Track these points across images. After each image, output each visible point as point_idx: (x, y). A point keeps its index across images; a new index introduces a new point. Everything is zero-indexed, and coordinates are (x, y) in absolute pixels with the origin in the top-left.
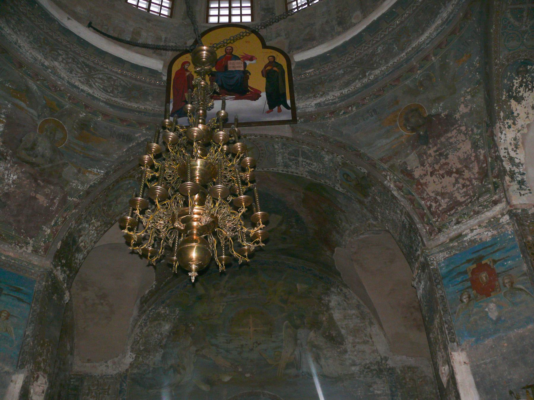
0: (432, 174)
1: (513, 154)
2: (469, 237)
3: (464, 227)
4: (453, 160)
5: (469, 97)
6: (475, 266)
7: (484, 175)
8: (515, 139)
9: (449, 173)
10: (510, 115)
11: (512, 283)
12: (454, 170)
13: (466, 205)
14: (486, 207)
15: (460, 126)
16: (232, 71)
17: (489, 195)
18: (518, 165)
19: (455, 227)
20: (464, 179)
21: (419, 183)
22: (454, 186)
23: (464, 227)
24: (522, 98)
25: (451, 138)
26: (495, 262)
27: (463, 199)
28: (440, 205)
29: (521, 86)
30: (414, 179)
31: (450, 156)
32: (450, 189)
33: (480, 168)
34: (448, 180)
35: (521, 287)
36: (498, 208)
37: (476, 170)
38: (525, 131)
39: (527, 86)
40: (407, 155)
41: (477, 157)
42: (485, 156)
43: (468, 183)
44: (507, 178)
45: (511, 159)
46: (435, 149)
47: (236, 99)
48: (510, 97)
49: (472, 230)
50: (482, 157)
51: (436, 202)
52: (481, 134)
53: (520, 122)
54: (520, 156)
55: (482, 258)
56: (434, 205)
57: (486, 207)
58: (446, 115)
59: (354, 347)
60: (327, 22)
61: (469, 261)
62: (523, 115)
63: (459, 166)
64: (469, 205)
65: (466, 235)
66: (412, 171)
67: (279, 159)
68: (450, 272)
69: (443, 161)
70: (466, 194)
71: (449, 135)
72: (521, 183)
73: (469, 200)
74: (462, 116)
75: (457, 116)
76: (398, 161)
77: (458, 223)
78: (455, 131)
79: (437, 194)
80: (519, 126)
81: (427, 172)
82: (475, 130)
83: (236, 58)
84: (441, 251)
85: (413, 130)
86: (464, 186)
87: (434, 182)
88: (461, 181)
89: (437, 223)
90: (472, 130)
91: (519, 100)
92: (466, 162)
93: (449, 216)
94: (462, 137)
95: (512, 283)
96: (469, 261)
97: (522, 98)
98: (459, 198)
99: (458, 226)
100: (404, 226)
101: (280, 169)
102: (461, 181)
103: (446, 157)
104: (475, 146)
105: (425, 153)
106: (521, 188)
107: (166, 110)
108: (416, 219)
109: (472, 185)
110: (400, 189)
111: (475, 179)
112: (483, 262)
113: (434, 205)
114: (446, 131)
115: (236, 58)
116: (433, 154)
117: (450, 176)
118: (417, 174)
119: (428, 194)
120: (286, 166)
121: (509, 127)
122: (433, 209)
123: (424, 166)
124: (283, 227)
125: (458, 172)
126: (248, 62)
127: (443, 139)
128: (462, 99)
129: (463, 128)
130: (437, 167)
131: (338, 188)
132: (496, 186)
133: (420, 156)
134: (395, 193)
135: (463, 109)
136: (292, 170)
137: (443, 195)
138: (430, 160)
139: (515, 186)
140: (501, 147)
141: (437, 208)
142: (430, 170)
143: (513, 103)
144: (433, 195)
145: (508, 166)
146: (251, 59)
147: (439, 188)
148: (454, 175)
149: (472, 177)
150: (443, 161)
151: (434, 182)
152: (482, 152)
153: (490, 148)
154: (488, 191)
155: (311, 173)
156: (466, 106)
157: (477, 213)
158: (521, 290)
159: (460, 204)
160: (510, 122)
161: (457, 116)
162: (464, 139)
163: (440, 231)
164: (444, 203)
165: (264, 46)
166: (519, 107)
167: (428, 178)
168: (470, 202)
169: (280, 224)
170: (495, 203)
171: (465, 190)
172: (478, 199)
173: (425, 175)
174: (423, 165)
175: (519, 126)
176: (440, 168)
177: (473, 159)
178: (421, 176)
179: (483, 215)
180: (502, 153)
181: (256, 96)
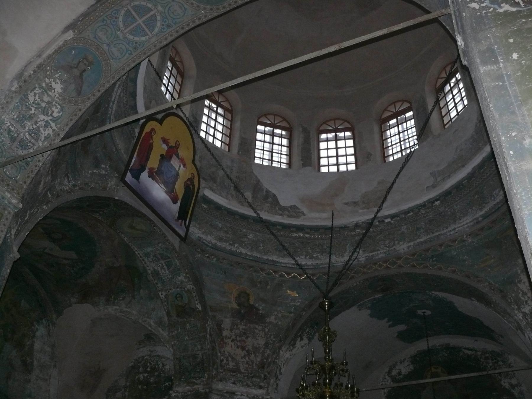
2: (239, 397)
3: (236, 389)
4: (250, 343)
5: (280, 315)
7: (262, 366)
9: (243, 348)
12: (247, 349)
13: (244, 376)
14: (255, 386)
15: (265, 327)
16: (172, 165)
17: (259, 380)
18: (280, 373)
19: (231, 385)
20: (249, 359)
21: (222, 340)
22: (242, 358)
23: (236, 389)
25: (257, 329)
27: (243, 371)
28: (228, 364)
30: (221, 335)
31: (249, 339)
34: (239, 352)
37: (259, 359)
40: (226, 317)
41: (263, 353)
42: (268, 355)
43: (251, 363)
46: (244, 327)
49: (242, 395)
50: (266, 355)
51: (227, 360)
52: (274, 342)
53: (294, 351)
56: (225, 361)
58: (262, 314)
59: (37, 380)
63: (251, 349)
64: (246, 377)
65: (237, 395)
66: (223, 329)
71: (257, 327)
73: (247, 374)
74: (270, 323)
75: (268, 320)
77: (234, 383)
78: (261, 327)
79: (230, 355)
81: (231, 337)
82: (272, 337)
84: (217, 394)
85: (239, 305)
86: (247, 363)
87: (231, 347)
88: (247, 358)
89: (222, 374)
90: (271, 335)
92: (256, 349)
93: (231, 375)
98: (241, 368)
99: (234, 386)
102: (247, 358)
103: (247, 337)
104: (266, 345)
105: (237, 325)
109: (253, 366)
111: (256, 364)
113: (225, 361)
116: (241, 329)
117: (242, 351)
118: (225, 333)
119: (224, 351)
122: (223, 363)
123: (231, 332)
125: (248, 351)
127: (252, 326)
128: (276, 313)
129: (267, 330)
130: (238, 339)
132: (265, 378)
135: (273, 318)
137: (232, 358)
138: (237, 331)
142: (234, 337)
144: (227, 354)
148: (245, 351)
149: (255, 361)
151: (231, 347)
152: (268, 352)
153: (274, 353)
154: (259, 377)
156: (276, 319)
157: (248, 386)
159: (241, 373)
161: (268, 320)
162: (263, 336)
163: (221, 380)
164: (231, 365)
167: (229, 341)
168: (247, 376)
170: (261, 387)
171: (247, 366)
172: (252, 377)
173: (229, 338)
174: (231, 330)
176: (240, 341)
177: (261, 351)
178: (226, 337)
179: (250, 390)
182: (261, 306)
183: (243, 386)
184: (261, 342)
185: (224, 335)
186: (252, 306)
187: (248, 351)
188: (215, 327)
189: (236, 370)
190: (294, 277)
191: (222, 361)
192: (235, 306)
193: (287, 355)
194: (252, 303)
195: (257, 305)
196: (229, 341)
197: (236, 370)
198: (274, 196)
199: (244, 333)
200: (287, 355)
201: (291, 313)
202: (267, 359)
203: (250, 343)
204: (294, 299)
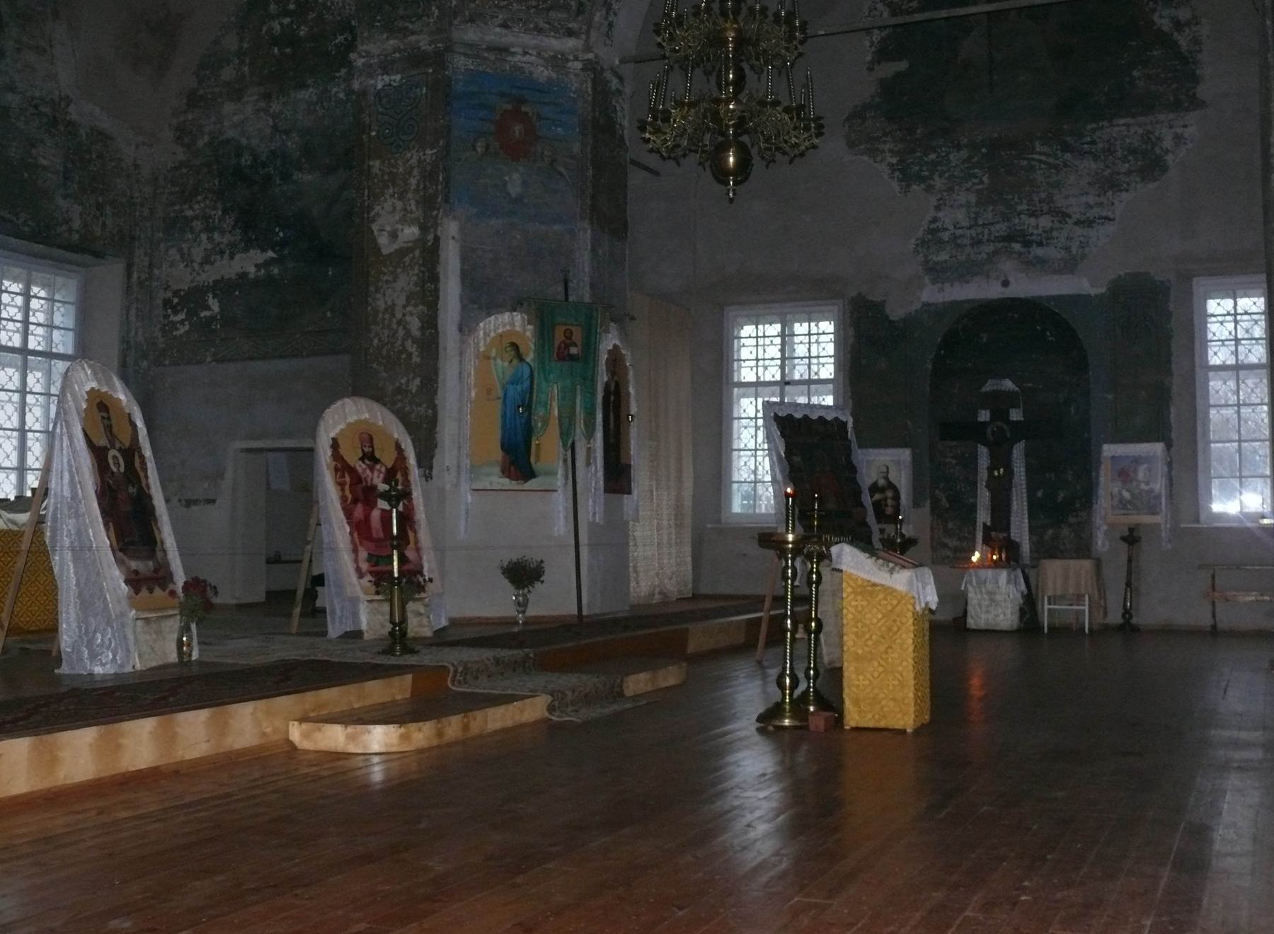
2: (518, 58)
6: (509, 107)
11: (553, 161)
13: (529, 8)
19: (498, 30)
26: (540, 117)
35: (563, 170)
49: (525, 53)
55: (523, 101)
61: (502, 95)
64: (532, 11)
65: (514, 54)
77: (504, 25)
95: (553, 161)
96: (502, 95)
99: (504, 31)
112: (523, 109)
158: (561, 174)
183: (526, 31)
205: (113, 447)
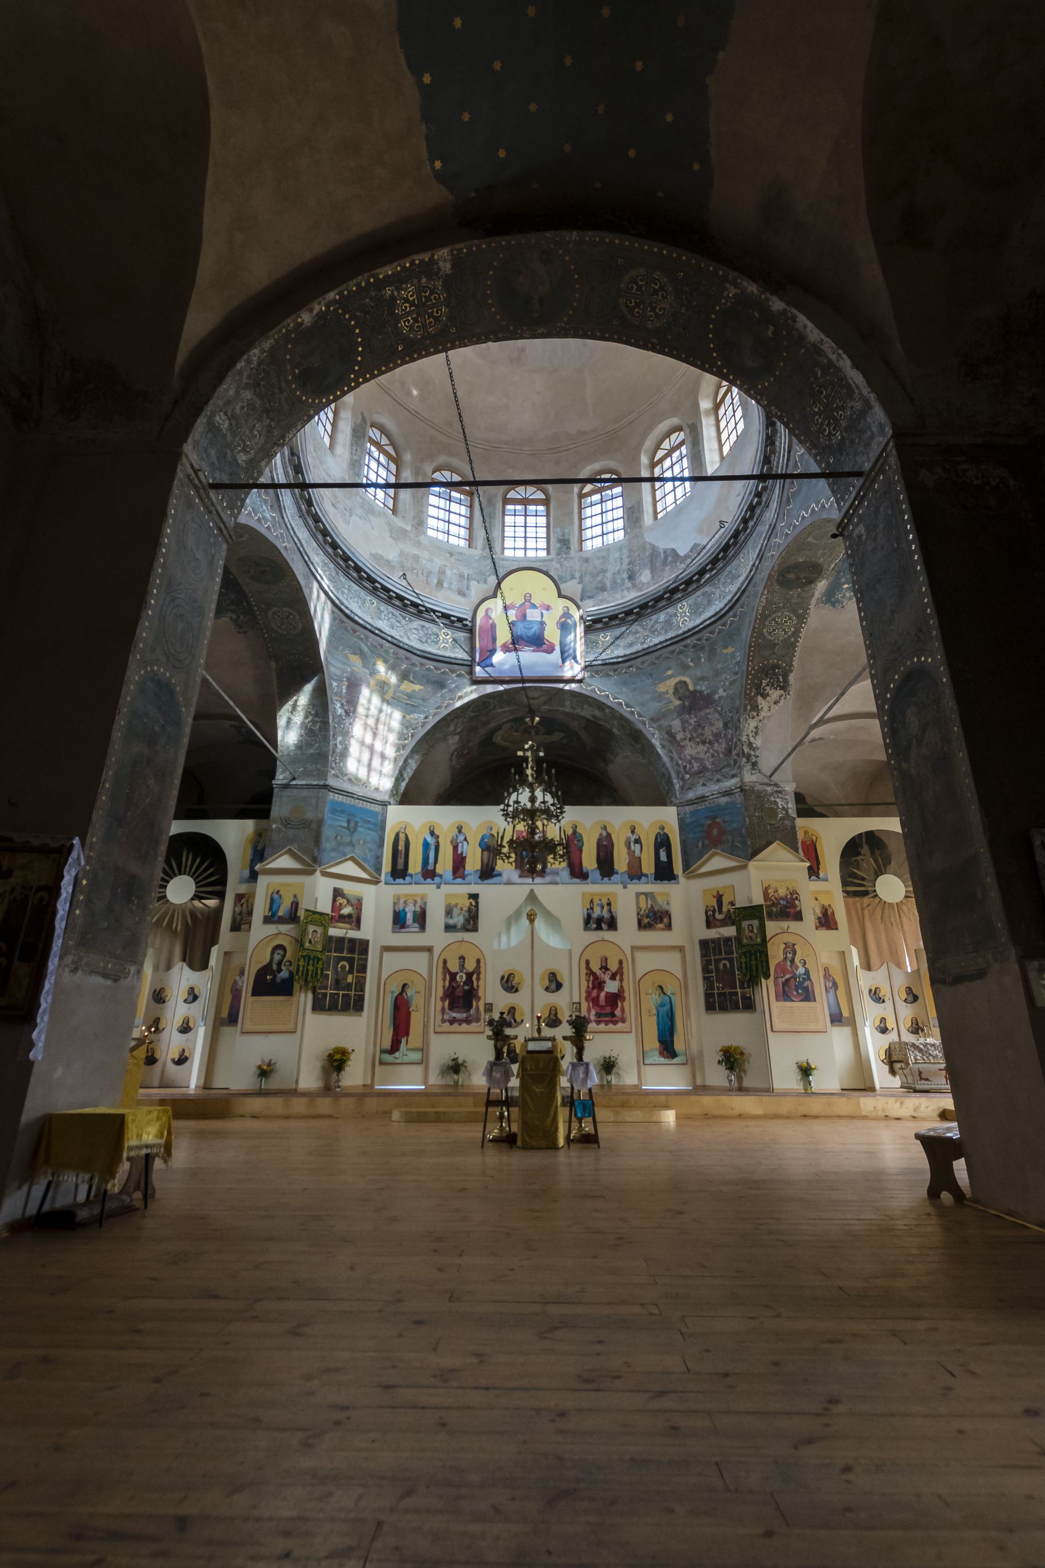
0: (690, 740)
1: (752, 740)
4: (708, 733)
7: (729, 751)
8: (756, 728)
9: (704, 742)
10: (756, 708)
11: (733, 842)
16: (531, 622)
18: (754, 750)
21: (679, 745)
24: (768, 695)
26: (725, 822)
27: (710, 767)
29: (768, 685)
32: (702, 755)
33: (727, 744)
34: (702, 748)
36: (734, 781)
37: (724, 746)
38: (766, 721)
39: (773, 685)
40: (673, 720)
44: (744, 760)
45: (750, 744)
47: (534, 651)
48: (757, 694)
53: (763, 714)
54: (758, 742)
55: (716, 817)
57: (726, 777)
60: (619, 572)
61: (708, 817)
62: (766, 708)
67: (568, 703)
68: (693, 822)
69: (700, 731)
70: (713, 763)
72: (754, 765)
74: (720, 698)
75: (716, 697)
76: (665, 723)
77: (704, 785)
79: (692, 757)
80: (761, 717)
83: (534, 606)
85: (680, 699)
86: (713, 756)
91: (764, 696)
92: (717, 736)
94: (717, 716)
95: (733, 842)
96: (708, 817)
97: (768, 695)
100: (663, 775)
101: (568, 710)
104: (726, 725)
106: (753, 769)
107: (473, 660)
108: (673, 775)
110: (663, 747)
114: (706, 707)
115: (534, 606)
120: (573, 708)
121: (753, 718)
124: (565, 741)
125: (711, 743)
126: (545, 612)
127: (702, 713)
129: (719, 709)
130: (694, 735)
131: (615, 730)
132: (735, 762)
133: (683, 722)
134: (659, 750)
135: (721, 692)
136: (578, 711)
137: (696, 759)
138: (690, 728)
139: (749, 767)
140: (745, 733)
141: (690, 769)
142: (689, 736)
143: (759, 699)
145: (746, 750)
146: (548, 608)
147: (693, 752)
150: (700, 731)
154: (729, 765)
155: (593, 716)
156: (725, 691)
157: (718, 781)
159: (707, 770)
160: (755, 714)
161: (716, 697)
164: (696, 766)
165: (560, 596)
166: (763, 702)
167: (687, 742)
169: (563, 739)
170: (733, 776)
174: (684, 731)
175: (761, 717)
180: (744, 739)
181: (550, 650)
182: (703, 687)
184: (721, 725)
185: (678, 739)
186: (695, 691)
187: (711, 743)
188: (666, 736)
189: (703, 770)
190: (720, 631)
191: (685, 767)
192: (677, 702)
193: (753, 724)
194: (691, 688)
195: (698, 688)
196: (687, 742)
197: (703, 770)
198: (673, 550)
199: (699, 725)
200: (753, 724)
201: (736, 673)
202: (731, 740)
203: (708, 733)
204: (733, 655)
205: (461, 971)
